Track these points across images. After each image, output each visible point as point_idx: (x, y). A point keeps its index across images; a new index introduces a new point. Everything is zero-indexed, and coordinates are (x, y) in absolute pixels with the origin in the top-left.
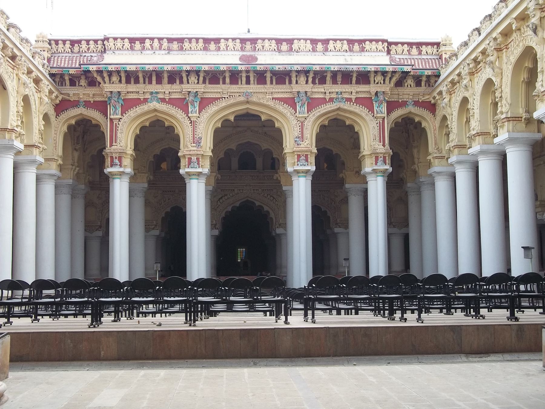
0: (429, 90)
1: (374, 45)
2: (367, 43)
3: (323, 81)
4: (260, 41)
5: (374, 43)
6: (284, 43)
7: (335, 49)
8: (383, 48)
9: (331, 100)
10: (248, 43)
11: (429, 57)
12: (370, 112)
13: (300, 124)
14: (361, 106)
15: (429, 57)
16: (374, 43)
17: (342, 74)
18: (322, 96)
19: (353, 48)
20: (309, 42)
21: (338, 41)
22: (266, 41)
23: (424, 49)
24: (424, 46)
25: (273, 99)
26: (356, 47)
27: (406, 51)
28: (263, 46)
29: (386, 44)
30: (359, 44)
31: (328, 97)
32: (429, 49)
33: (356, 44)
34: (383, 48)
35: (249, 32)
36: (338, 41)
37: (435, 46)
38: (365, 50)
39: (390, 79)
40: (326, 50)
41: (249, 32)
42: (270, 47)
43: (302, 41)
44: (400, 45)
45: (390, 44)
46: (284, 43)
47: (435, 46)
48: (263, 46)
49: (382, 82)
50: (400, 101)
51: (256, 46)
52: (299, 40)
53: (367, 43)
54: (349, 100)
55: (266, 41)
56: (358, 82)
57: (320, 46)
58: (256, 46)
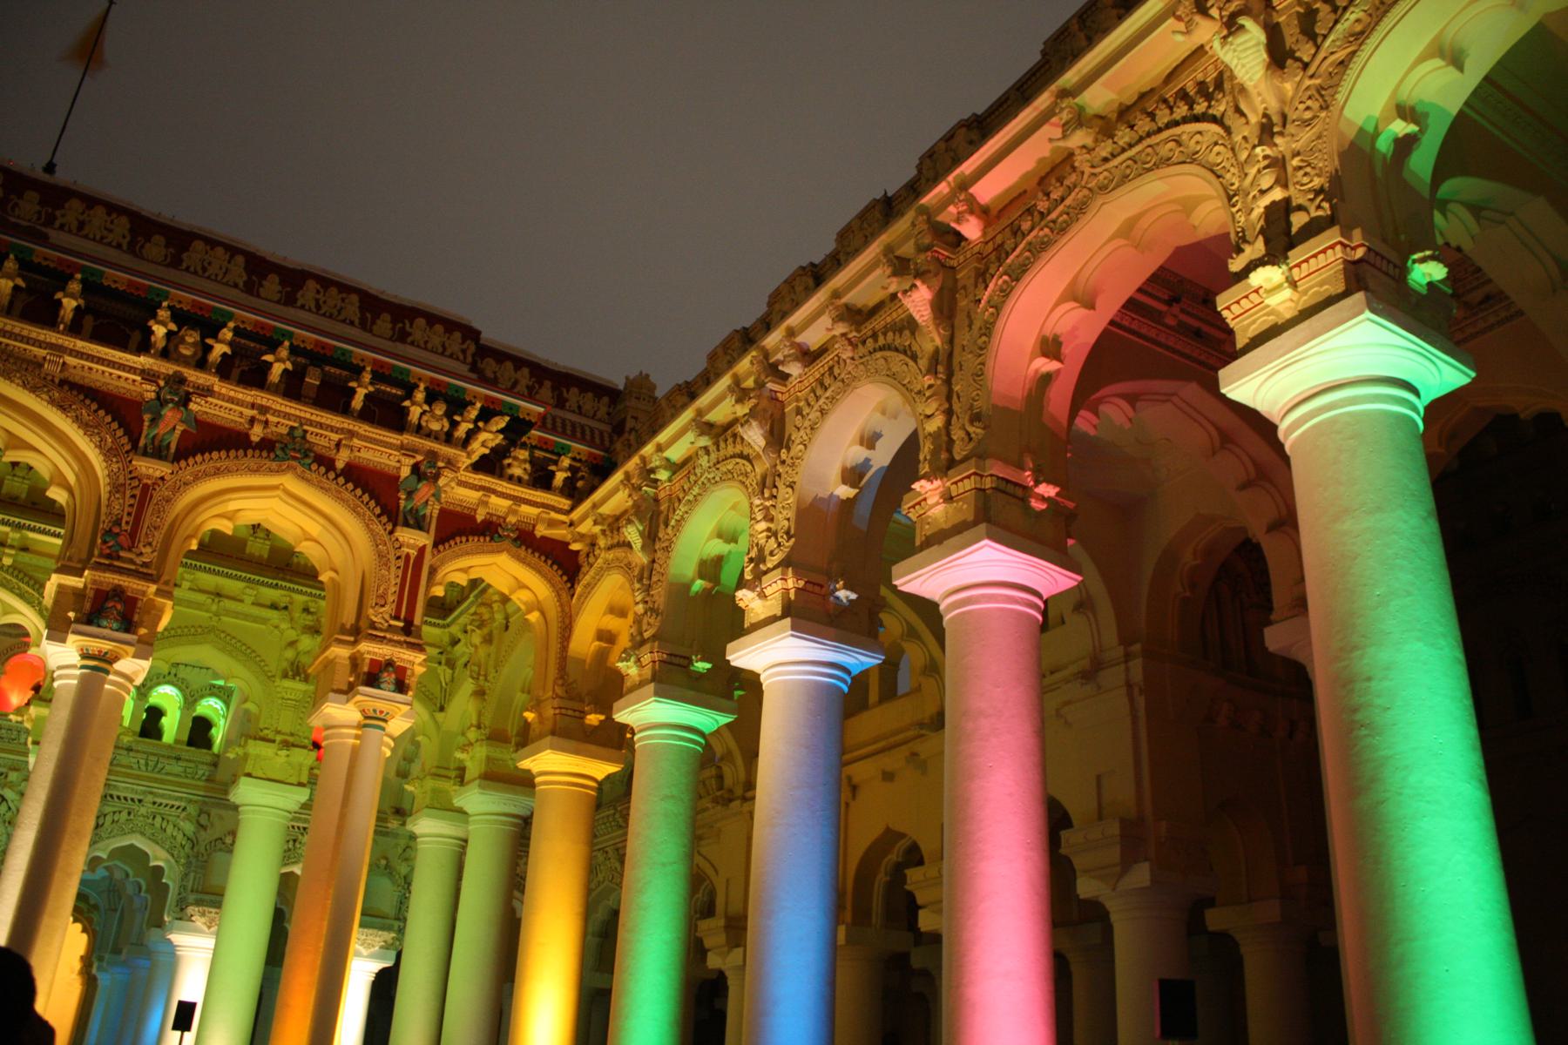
0: (565, 503)
1: (437, 336)
2: (421, 322)
3: (255, 377)
4: (75, 204)
5: (439, 328)
6: (159, 239)
7: (318, 307)
8: (464, 352)
9: (267, 445)
10: (32, 196)
11: (584, 421)
12: (384, 519)
13: (137, 492)
14: (359, 492)
15: (584, 421)
16: (439, 328)
17: (323, 382)
18: (241, 423)
19: (373, 323)
20: (240, 259)
21: (334, 291)
22: (100, 211)
23: (573, 395)
24: (574, 390)
25: (63, 382)
26: (384, 324)
27: (521, 388)
28: (81, 225)
29: (473, 348)
30: (394, 322)
31: (257, 433)
32: (588, 402)
33: (386, 317)
34: (464, 352)
35: (50, 168)
36: (334, 291)
37: (606, 399)
38: (410, 339)
39: (471, 435)
40: (290, 300)
41: (50, 168)
42: (105, 233)
43: (220, 250)
44: (509, 365)
45: (485, 351)
46: (159, 239)
47: (606, 399)
48: (81, 225)
49: (443, 437)
50: (479, 518)
51: (58, 213)
52: (212, 243)
53: (421, 322)
54: (326, 463)
55: (100, 211)
56: (366, 416)
57: (272, 285)
58: (58, 213)
